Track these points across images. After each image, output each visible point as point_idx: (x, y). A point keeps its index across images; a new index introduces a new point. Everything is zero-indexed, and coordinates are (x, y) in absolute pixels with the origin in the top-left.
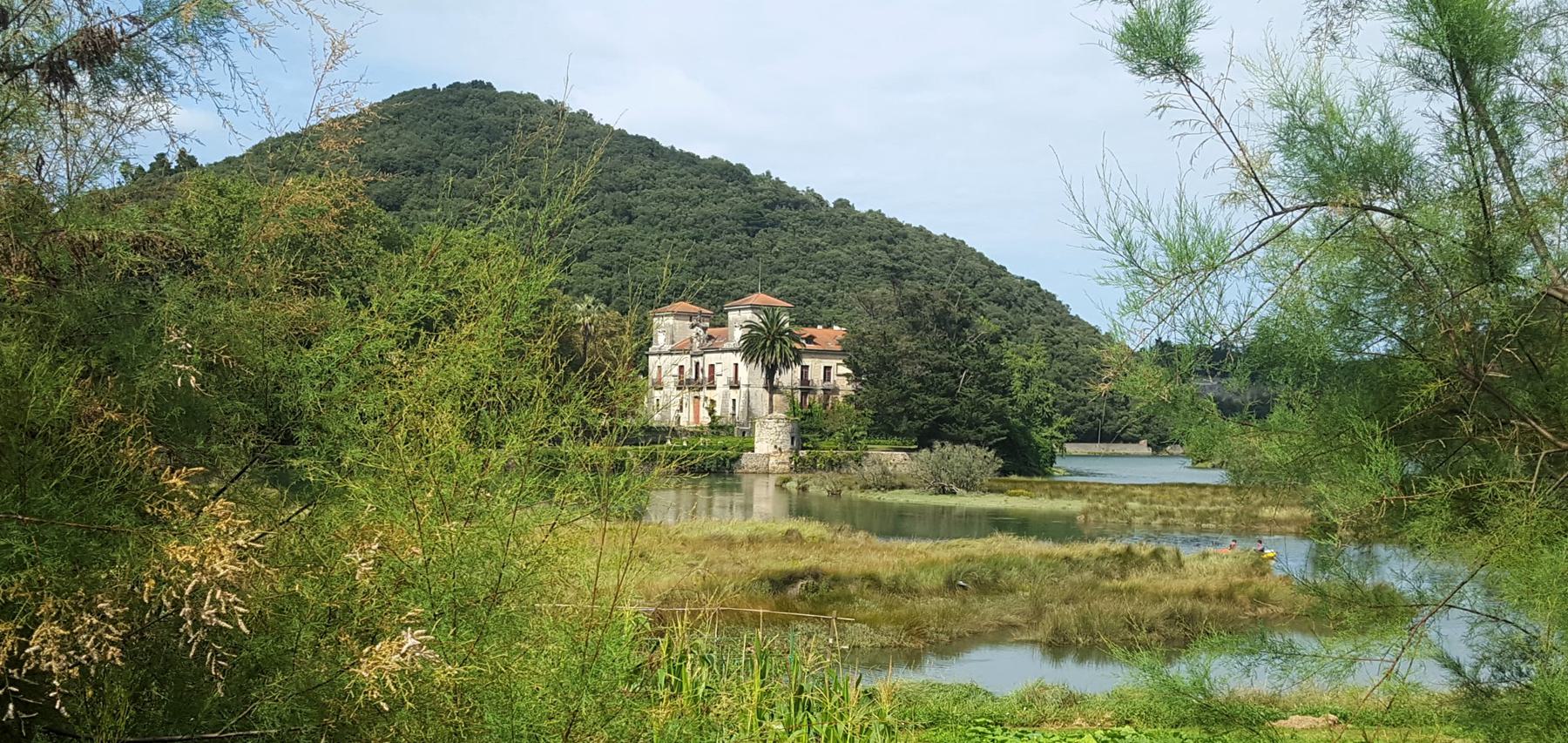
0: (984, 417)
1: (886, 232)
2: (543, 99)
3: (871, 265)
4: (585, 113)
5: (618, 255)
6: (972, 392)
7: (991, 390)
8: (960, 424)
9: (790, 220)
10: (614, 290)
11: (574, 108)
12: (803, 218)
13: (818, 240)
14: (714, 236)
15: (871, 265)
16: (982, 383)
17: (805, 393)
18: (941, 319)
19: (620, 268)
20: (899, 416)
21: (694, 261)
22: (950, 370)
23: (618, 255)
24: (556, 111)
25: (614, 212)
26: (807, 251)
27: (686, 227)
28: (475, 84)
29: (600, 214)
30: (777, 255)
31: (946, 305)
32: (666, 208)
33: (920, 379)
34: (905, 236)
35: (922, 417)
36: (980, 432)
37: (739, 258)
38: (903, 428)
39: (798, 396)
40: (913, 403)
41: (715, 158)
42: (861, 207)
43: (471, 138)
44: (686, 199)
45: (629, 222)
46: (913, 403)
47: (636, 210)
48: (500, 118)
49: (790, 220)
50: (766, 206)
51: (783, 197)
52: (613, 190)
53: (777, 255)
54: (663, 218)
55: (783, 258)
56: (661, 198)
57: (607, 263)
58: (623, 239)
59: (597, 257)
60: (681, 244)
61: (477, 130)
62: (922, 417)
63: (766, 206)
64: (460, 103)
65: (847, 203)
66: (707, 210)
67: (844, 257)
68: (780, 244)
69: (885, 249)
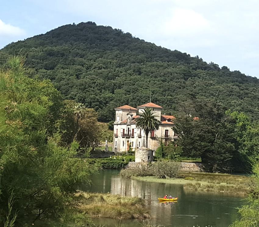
0: (223, 151)
1: (240, 79)
2: (114, 28)
3: (232, 92)
4: (129, 33)
5: (133, 87)
6: (219, 141)
7: (227, 140)
8: (214, 153)
9: (202, 74)
10: (130, 100)
11: (125, 32)
12: (207, 74)
13: (212, 82)
14: (171, 80)
15: (232, 92)
16: (224, 138)
17: (166, 140)
18: (210, 113)
19: (133, 92)
20: (191, 149)
21: (162, 90)
22: (212, 132)
23: (133, 87)
24: (118, 33)
25: (134, 71)
26: (207, 86)
27: (161, 77)
28: (89, 22)
29: (128, 72)
30: (195, 87)
31: (212, 109)
32: (153, 69)
33: (199, 136)
34: (247, 81)
35: (199, 150)
36: (222, 156)
37: (180, 88)
38: (192, 154)
39: (164, 141)
40: (196, 145)
41: (176, 50)
42: (232, 69)
43: (84, 43)
44: (162, 66)
45: (139, 75)
46: (196, 145)
47: (142, 70)
48: (96, 35)
49: (202, 74)
50: (193, 69)
51: (200, 65)
52: (134, 62)
53: (195, 87)
54: (152, 73)
55: (197, 88)
56: (153, 65)
57: (128, 90)
58: (136, 80)
59: (125, 87)
60: (158, 83)
61: (86, 40)
62: (199, 150)
63: (193, 69)
64: (81, 30)
65: (226, 67)
66: (169, 70)
67: (221, 88)
68: (197, 83)
69: (237, 85)
